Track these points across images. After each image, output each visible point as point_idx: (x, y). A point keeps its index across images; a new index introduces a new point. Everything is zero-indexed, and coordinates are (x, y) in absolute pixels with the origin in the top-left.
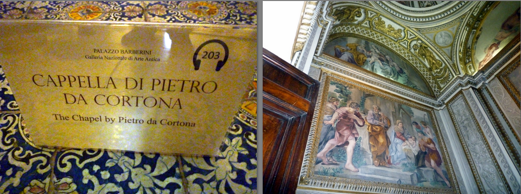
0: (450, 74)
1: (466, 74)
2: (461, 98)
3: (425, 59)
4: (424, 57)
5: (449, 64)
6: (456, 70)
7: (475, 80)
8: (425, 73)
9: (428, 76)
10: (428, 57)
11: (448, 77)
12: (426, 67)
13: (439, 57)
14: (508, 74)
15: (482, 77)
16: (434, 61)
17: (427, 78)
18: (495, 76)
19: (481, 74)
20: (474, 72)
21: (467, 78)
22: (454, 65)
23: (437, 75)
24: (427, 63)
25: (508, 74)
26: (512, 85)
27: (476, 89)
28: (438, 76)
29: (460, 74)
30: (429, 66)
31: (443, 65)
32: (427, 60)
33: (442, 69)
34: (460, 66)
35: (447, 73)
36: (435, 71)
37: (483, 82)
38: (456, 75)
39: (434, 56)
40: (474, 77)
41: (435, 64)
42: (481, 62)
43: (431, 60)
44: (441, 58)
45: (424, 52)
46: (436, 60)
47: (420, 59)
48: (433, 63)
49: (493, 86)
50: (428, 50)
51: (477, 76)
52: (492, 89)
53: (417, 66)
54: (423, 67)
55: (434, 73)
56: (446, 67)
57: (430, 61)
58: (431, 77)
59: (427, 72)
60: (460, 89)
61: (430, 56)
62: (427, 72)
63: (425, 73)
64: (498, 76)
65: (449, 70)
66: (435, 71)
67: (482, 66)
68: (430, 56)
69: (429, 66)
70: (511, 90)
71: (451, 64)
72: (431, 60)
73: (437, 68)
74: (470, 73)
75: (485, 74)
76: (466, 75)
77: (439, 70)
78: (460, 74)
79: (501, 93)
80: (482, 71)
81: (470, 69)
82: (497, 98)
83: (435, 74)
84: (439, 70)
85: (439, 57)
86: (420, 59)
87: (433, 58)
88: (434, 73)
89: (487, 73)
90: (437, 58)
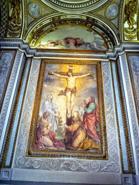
0: (19, 34)
1: (28, 43)
2: (13, 53)
3: (12, 9)
4: (13, 6)
5: (24, 28)
6: (25, 36)
7: (30, 51)
8: (4, 17)
9: (4, 21)
10: (15, 10)
11: (17, 34)
12: (8, 14)
13: (22, 17)
14: (47, 63)
15: (34, 53)
16: (17, 16)
17: (2, 21)
18: (41, 59)
19: (35, 51)
20: (33, 47)
21: (27, 46)
22: (26, 31)
23: (10, 26)
24: (11, 12)
25: (47, 63)
26: (44, 70)
27: (26, 56)
28: (11, 28)
29: (25, 40)
30: (10, 15)
31: (20, 25)
32: (13, 10)
33: (17, 26)
34: (29, 36)
35: (18, 31)
36: (12, 23)
37: (33, 56)
38: (22, 38)
39: (19, 13)
40: (30, 49)
41: (16, 18)
42: (41, 45)
43: (16, 13)
44: (22, 19)
45: (15, 3)
46: (18, 17)
47: (10, 5)
48: (15, 17)
49: (36, 62)
50: (19, 5)
51: (32, 50)
52: (34, 64)
53: (2, 6)
54: (6, 12)
55: (10, 23)
56: (20, 28)
57: (15, 13)
58: (6, 23)
59: (6, 17)
60: (17, 48)
61: (17, 11)
62: (6, 17)
63: (4, 17)
64: (42, 60)
65: (21, 32)
66: (12, 23)
67: (40, 47)
68: (17, 11)
69: (10, 15)
70: (42, 71)
71: (26, 29)
72: (16, 13)
73: (14, 22)
74: (31, 45)
75: (37, 53)
76: (28, 44)
77: (15, 25)
78: (25, 40)
79: (36, 69)
80: (38, 50)
81: (33, 43)
82: (32, 70)
83: (10, 24)
84: (15, 25)
85: (22, 17)
86: (10, 5)
87: (18, 14)
88: (10, 23)
89: (38, 53)
90: (21, 16)
